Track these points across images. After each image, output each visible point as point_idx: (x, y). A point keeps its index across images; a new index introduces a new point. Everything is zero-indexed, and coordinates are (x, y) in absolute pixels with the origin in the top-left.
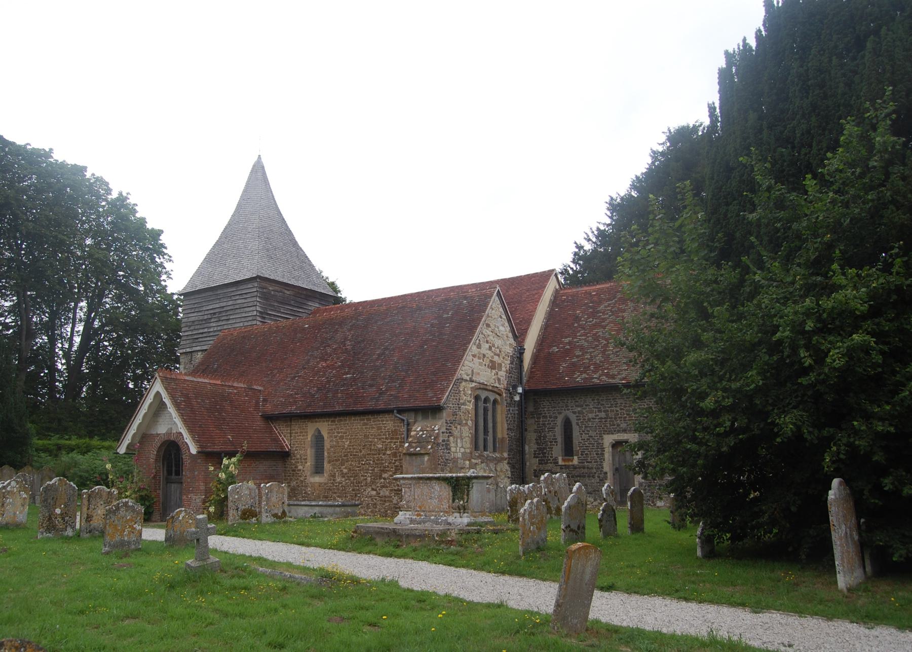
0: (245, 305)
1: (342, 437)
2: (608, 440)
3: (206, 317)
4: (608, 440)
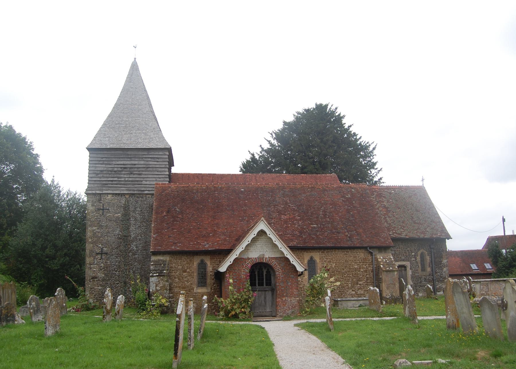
0: (157, 166)
1: (330, 262)
3: (116, 169)
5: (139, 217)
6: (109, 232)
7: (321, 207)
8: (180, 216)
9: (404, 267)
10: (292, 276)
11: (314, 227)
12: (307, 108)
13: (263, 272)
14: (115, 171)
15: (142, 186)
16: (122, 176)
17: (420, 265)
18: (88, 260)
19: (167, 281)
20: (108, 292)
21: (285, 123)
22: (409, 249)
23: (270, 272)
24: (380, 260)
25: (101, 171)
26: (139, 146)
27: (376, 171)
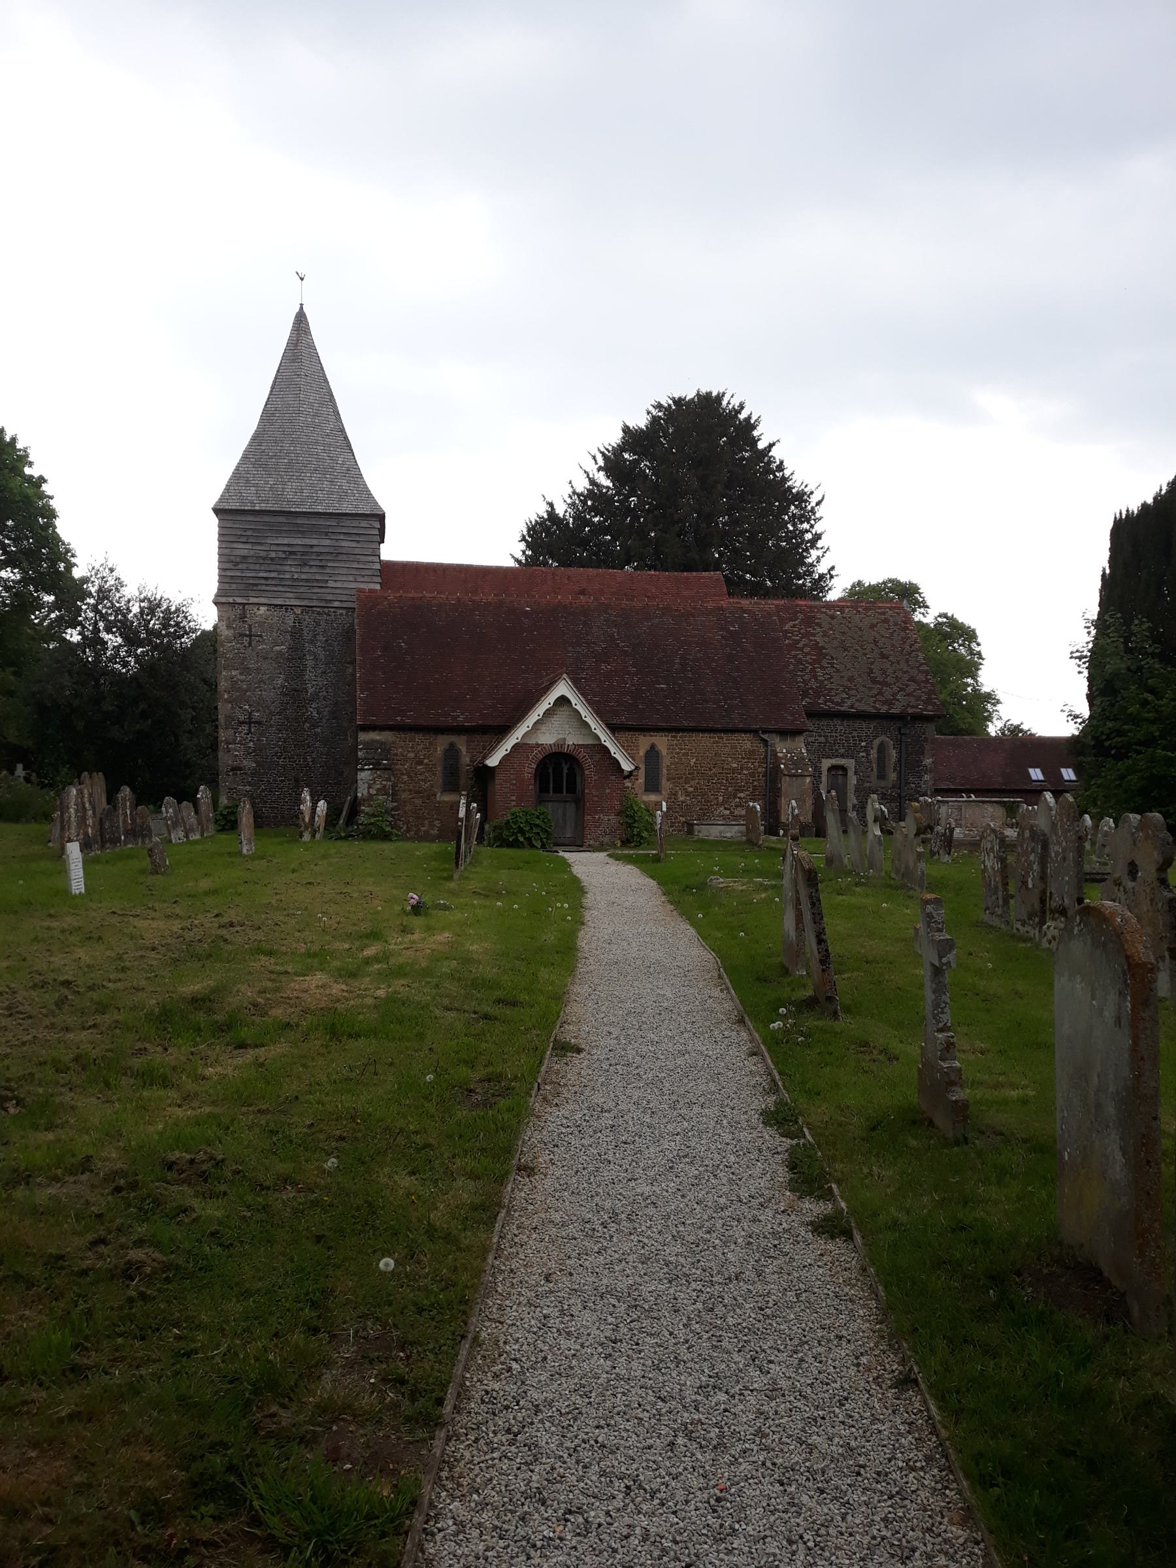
0: (357, 551)
2: (826, 763)
3: (273, 555)
4: (826, 763)
5: (322, 654)
6: (261, 681)
8: (408, 658)
9: (844, 769)
10: (613, 778)
12: (677, 396)
14: (272, 559)
15: (328, 591)
16: (287, 568)
17: (875, 766)
18: (223, 735)
19: (388, 780)
20: (306, 795)
21: (626, 430)
22: (855, 734)
24: (780, 755)
25: (244, 557)
26: (320, 509)
27: (820, 553)
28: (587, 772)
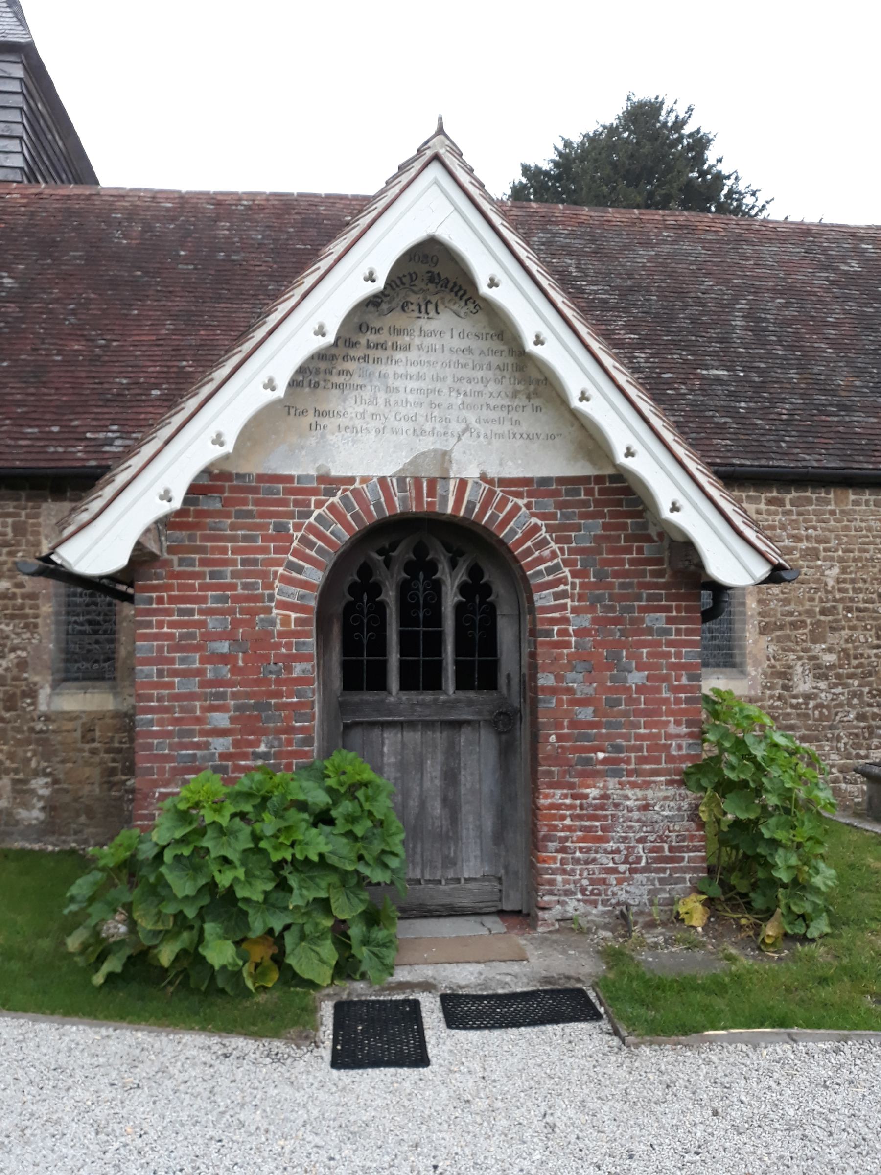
1: (813, 554)
7: (736, 299)
11: (718, 380)
13: (437, 587)
23: (487, 590)
28: (543, 599)
